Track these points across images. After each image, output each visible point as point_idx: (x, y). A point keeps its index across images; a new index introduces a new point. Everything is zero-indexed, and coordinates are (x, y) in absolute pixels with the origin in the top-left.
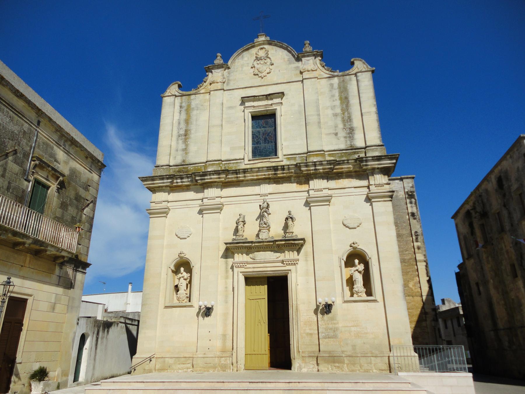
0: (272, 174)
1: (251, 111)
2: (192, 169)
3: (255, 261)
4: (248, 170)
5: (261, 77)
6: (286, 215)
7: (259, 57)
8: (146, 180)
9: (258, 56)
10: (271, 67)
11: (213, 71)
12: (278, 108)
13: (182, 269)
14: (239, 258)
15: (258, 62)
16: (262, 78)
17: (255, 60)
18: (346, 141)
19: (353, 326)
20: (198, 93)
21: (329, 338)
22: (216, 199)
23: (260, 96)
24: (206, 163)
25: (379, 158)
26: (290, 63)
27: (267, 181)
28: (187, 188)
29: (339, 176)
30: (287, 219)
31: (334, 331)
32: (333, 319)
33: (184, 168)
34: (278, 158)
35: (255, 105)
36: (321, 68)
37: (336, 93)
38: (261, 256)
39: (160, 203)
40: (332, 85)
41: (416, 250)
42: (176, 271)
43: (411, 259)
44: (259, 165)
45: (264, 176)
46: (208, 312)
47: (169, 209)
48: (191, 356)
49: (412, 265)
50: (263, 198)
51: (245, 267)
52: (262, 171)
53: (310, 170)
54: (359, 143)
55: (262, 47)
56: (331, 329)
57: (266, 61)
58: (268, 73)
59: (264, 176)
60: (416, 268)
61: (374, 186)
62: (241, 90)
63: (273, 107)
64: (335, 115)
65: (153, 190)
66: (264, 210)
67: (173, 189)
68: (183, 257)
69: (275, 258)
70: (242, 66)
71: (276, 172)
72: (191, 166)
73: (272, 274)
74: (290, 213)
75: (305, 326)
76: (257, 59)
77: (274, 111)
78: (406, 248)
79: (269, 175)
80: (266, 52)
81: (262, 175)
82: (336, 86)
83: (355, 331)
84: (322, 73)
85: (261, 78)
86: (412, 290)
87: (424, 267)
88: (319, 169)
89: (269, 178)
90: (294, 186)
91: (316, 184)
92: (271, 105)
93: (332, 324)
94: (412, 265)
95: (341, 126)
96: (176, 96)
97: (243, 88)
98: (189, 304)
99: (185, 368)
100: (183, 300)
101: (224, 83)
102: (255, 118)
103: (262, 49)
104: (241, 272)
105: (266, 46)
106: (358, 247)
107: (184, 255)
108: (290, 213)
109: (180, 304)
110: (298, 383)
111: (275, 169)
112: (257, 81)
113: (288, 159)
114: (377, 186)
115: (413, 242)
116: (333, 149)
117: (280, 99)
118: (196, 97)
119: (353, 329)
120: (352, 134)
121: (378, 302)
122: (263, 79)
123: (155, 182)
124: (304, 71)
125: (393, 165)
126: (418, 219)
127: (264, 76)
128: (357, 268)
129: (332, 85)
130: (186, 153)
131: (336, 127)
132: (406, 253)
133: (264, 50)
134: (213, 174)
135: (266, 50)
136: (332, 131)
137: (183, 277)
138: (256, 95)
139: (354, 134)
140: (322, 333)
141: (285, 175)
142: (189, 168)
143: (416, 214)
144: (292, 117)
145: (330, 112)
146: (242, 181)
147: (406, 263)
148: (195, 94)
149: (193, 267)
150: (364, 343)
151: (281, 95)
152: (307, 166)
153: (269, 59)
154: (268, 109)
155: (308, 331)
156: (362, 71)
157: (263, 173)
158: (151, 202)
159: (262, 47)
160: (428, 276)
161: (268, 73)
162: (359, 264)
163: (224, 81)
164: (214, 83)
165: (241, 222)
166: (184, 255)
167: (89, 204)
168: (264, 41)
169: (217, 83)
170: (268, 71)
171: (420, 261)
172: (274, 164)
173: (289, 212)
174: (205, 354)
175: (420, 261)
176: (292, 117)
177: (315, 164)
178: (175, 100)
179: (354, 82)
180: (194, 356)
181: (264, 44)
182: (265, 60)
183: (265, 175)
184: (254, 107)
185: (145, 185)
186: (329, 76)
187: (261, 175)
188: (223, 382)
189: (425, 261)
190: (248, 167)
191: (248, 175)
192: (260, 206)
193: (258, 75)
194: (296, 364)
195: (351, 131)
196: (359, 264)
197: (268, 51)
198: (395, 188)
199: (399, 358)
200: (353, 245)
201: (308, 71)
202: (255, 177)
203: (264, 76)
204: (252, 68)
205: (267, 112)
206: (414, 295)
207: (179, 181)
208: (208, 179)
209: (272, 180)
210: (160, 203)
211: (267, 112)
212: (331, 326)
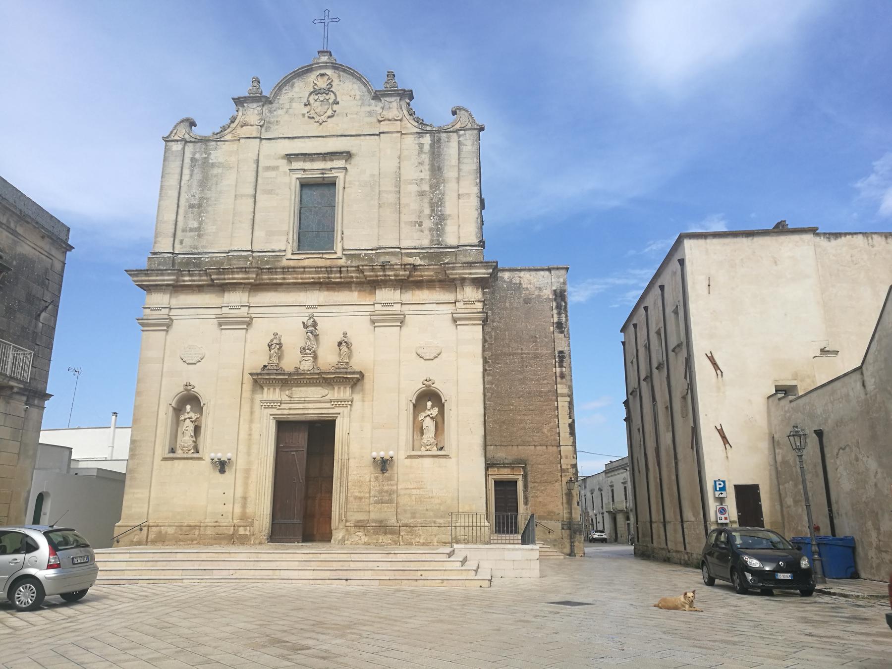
0: (323, 278)
1: (300, 176)
2: (207, 260)
3: (292, 399)
4: (290, 270)
5: (318, 122)
6: (340, 337)
7: (317, 88)
8: (136, 275)
9: (316, 87)
10: (335, 107)
11: (245, 105)
12: (340, 175)
13: (188, 407)
14: (271, 394)
15: (316, 97)
16: (321, 124)
17: (310, 94)
18: (432, 235)
19: (415, 488)
20: (222, 139)
21: (382, 503)
22: (242, 308)
23: (315, 154)
24: (229, 252)
25: (470, 265)
26: (362, 105)
27: (318, 286)
28: (200, 289)
29: (419, 284)
30: (340, 344)
31: (390, 494)
32: (390, 479)
33: (195, 258)
34: (336, 253)
35: (306, 168)
36: (408, 117)
37: (426, 158)
38: (300, 392)
39: (159, 309)
40: (421, 145)
41: (558, 379)
42: (178, 410)
43: (550, 391)
44: (306, 263)
45: (313, 280)
46: (222, 466)
47: (172, 320)
48: (198, 524)
49: (551, 400)
50: (310, 311)
51: (279, 407)
52: (310, 273)
53: (377, 276)
54: (451, 239)
55: (323, 71)
56: (387, 492)
57: (327, 97)
58: (329, 117)
59: (313, 280)
60: (556, 405)
61: (462, 303)
62: (287, 140)
63: (333, 173)
64: (422, 194)
65: (148, 288)
66: (312, 328)
67: (177, 288)
68: (190, 390)
69: (320, 396)
70: (292, 100)
71: (330, 276)
72: (207, 256)
73: (315, 417)
74: (345, 334)
75: (354, 487)
76: (316, 92)
77: (334, 179)
78: (544, 375)
79: (319, 278)
80: (329, 81)
81: (309, 278)
82: (427, 148)
83: (417, 495)
84: (409, 125)
85: (318, 124)
86: (547, 437)
87: (567, 404)
88: (389, 276)
89: (320, 283)
90: (352, 296)
91: (385, 295)
92: (331, 169)
93: (388, 485)
94: (551, 400)
95: (427, 211)
96: (186, 142)
97: (289, 138)
98: (196, 455)
99: (189, 540)
100: (189, 450)
101: (261, 126)
102: (304, 185)
103: (322, 75)
104: (271, 415)
105: (329, 72)
106: (433, 385)
107: (191, 387)
108: (345, 334)
109: (185, 455)
110: (319, 555)
111: (329, 269)
112: (313, 129)
113: (349, 257)
114: (466, 303)
115: (555, 367)
116: (413, 245)
117: (344, 161)
118: (217, 145)
119: (414, 492)
120: (441, 225)
121: (450, 458)
122: (321, 126)
123: (151, 278)
124: (382, 119)
125: (489, 276)
126: (565, 333)
127: (323, 122)
128: (429, 413)
129: (421, 145)
130: (199, 236)
131: (421, 212)
132: (544, 382)
133: (327, 77)
134: (238, 273)
135: (329, 79)
136: (414, 218)
137: (189, 418)
138: (308, 152)
139: (445, 224)
140: (374, 497)
141: (343, 280)
142: (202, 259)
143: (564, 326)
144: (360, 191)
145: (414, 188)
146: (281, 284)
147: (541, 397)
148: (217, 141)
149: (204, 404)
150: (427, 510)
151: (347, 155)
152: (373, 270)
153: (332, 93)
154: (325, 176)
155: (357, 494)
156: (466, 128)
157: (311, 276)
158: (144, 308)
159: (323, 71)
160: (570, 418)
161: (329, 117)
162: (433, 407)
163: (260, 124)
164: (247, 125)
165: (276, 346)
166: (191, 387)
167: (47, 307)
168: (327, 63)
169: (251, 125)
170: (329, 113)
171: (563, 395)
172: (328, 263)
173: (343, 334)
174: (216, 522)
175: (563, 395)
176: (360, 191)
177: (383, 267)
178: (184, 148)
179: (454, 145)
180: (202, 524)
181: (326, 67)
182: (327, 94)
183: (313, 278)
184: (304, 170)
185: (135, 281)
186: (418, 130)
187: (309, 277)
188: (230, 553)
189: (569, 396)
190: (292, 263)
191: (290, 276)
192: (303, 323)
193: (313, 118)
194: (338, 535)
195: (440, 220)
196: (433, 407)
197: (332, 81)
198: (538, 283)
199: (466, 528)
200: (425, 382)
201: (389, 120)
202: (300, 281)
203: (323, 122)
204: (306, 105)
205: (324, 180)
206: (549, 444)
207: (187, 278)
208: (229, 279)
209: (324, 286)
210: (159, 309)
211: (324, 180)
212: (386, 488)
